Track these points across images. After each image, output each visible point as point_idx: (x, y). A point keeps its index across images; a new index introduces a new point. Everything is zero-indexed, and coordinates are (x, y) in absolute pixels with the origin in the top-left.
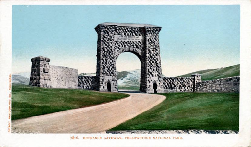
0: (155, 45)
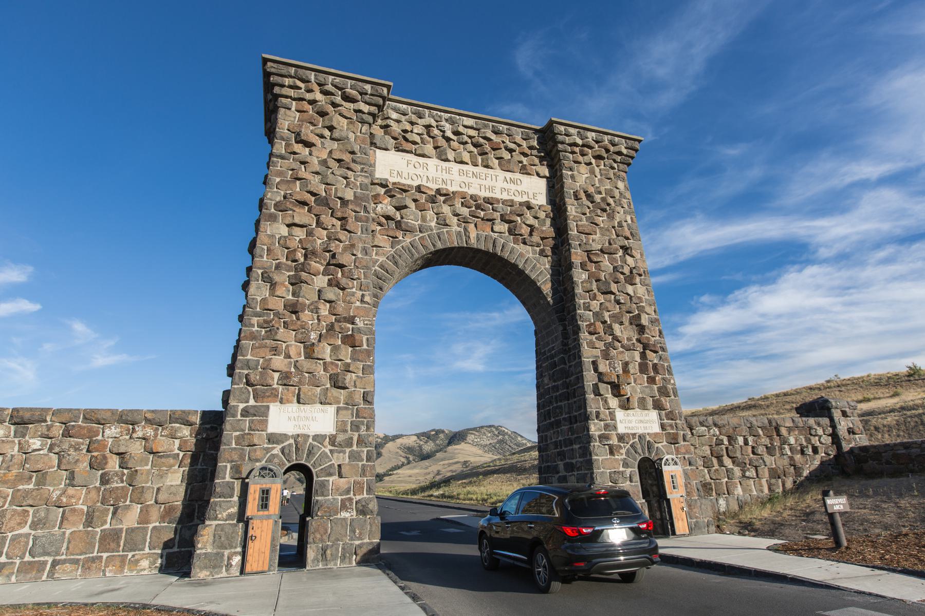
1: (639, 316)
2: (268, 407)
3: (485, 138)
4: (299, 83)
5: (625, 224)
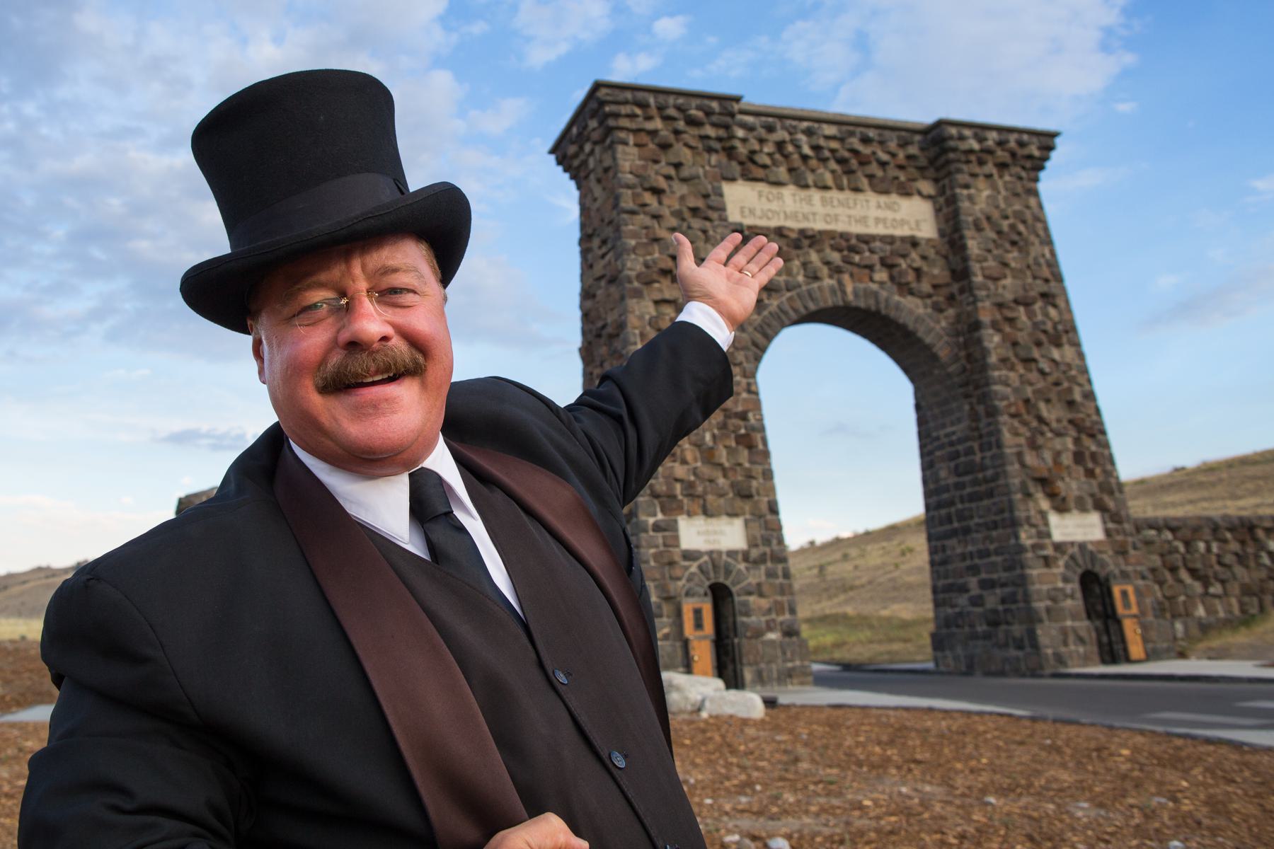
1: (1070, 390)
2: (676, 522)
5: (1042, 261)
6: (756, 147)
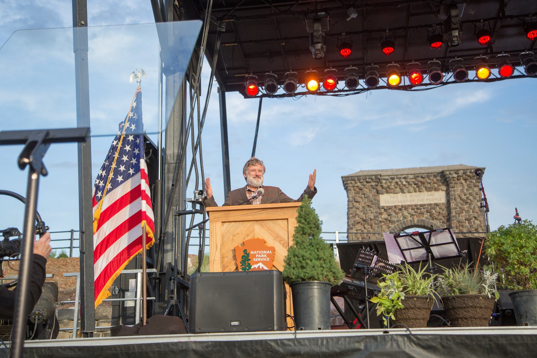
0: (472, 206)
3: (418, 181)
4: (353, 182)
6: (389, 184)
